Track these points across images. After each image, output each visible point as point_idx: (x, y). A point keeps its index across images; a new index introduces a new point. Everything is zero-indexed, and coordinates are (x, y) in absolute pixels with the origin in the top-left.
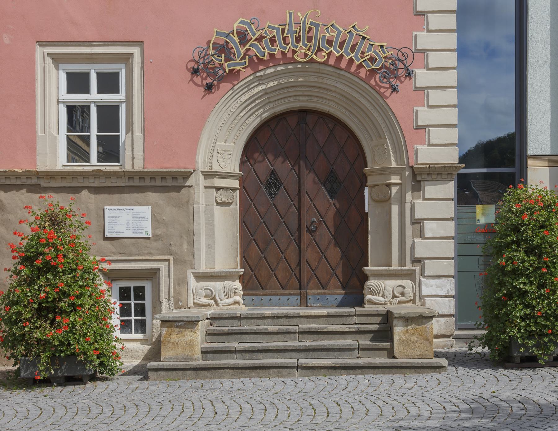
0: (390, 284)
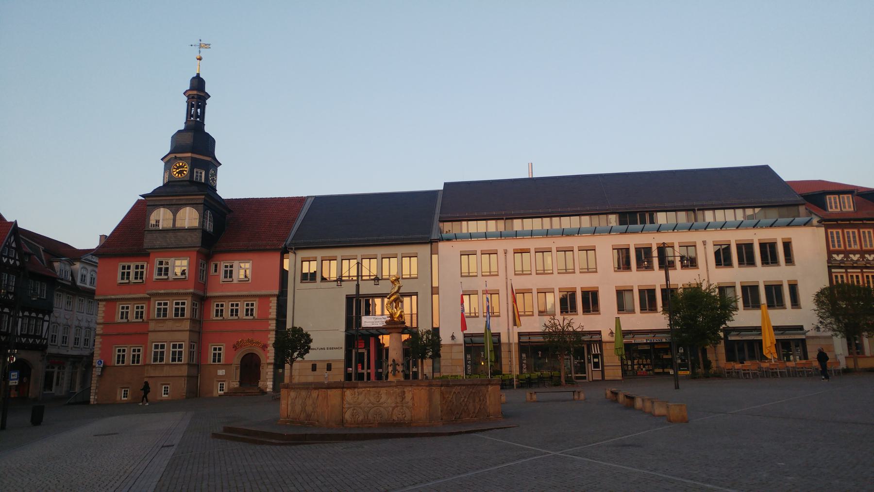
0: (262, 383)
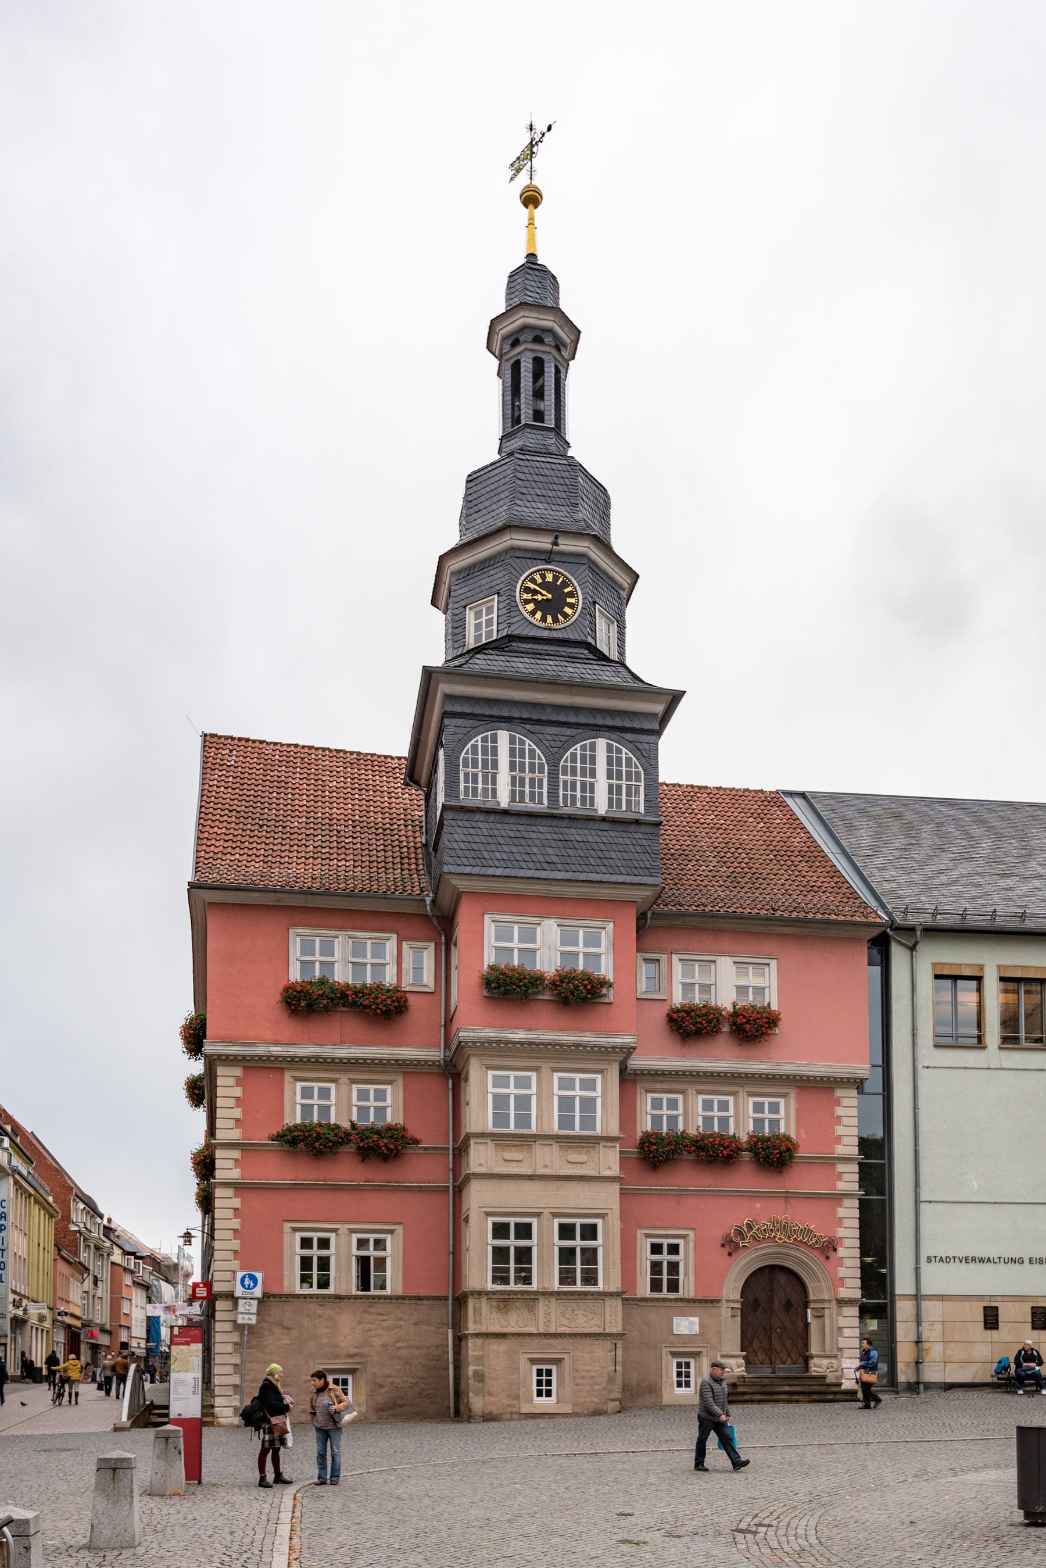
0: (825, 1362)
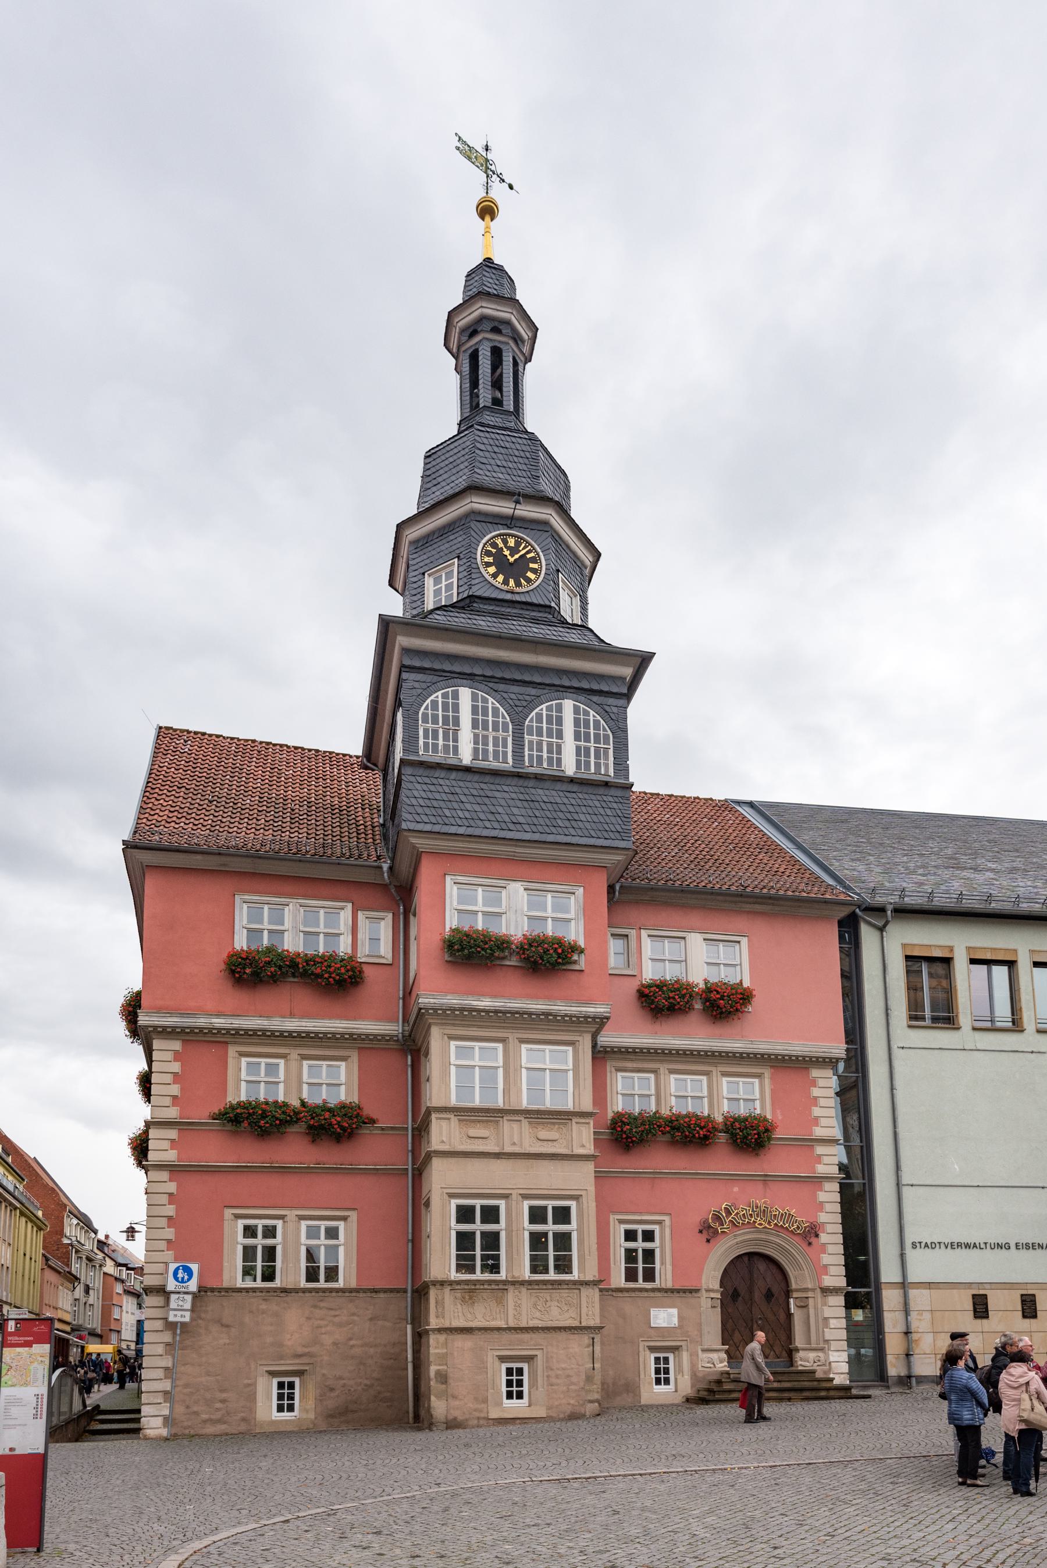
0: (812, 1355)
